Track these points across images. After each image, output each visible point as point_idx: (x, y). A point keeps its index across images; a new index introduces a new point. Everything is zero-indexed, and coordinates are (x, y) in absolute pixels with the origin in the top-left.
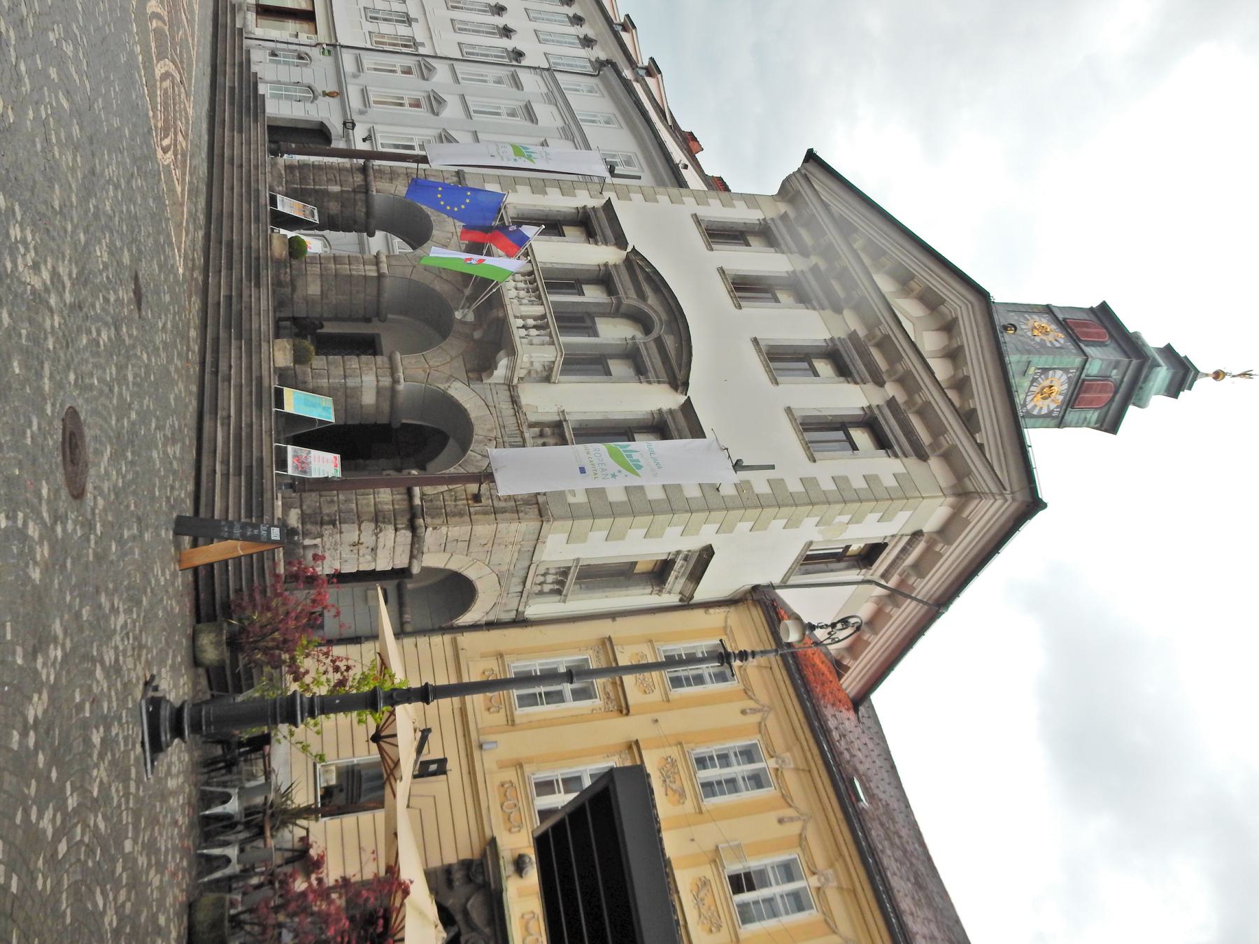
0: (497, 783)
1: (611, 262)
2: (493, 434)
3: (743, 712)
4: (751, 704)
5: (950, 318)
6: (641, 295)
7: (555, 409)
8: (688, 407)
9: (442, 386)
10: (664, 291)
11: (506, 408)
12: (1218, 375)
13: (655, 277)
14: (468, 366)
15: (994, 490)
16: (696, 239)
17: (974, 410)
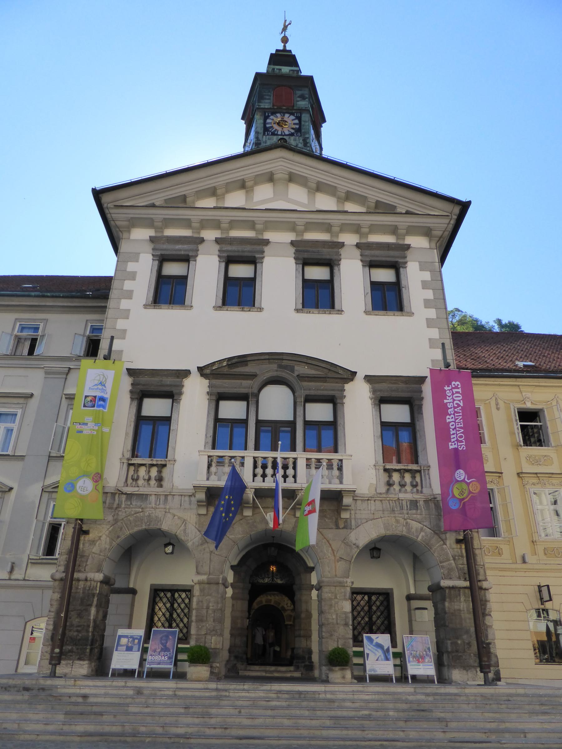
0: (545, 557)
1: (208, 390)
2: (401, 520)
3: (498, 409)
4: (493, 403)
5: (287, 176)
6: (253, 376)
7: (373, 471)
8: (369, 379)
9: (355, 551)
10: (249, 359)
11: (373, 506)
12: (285, 40)
13: (234, 361)
14: (334, 527)
15: (447, 221)
16: (168, 315)
17: (377, 201)
